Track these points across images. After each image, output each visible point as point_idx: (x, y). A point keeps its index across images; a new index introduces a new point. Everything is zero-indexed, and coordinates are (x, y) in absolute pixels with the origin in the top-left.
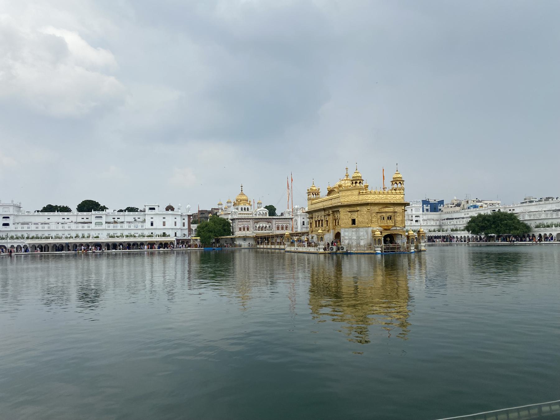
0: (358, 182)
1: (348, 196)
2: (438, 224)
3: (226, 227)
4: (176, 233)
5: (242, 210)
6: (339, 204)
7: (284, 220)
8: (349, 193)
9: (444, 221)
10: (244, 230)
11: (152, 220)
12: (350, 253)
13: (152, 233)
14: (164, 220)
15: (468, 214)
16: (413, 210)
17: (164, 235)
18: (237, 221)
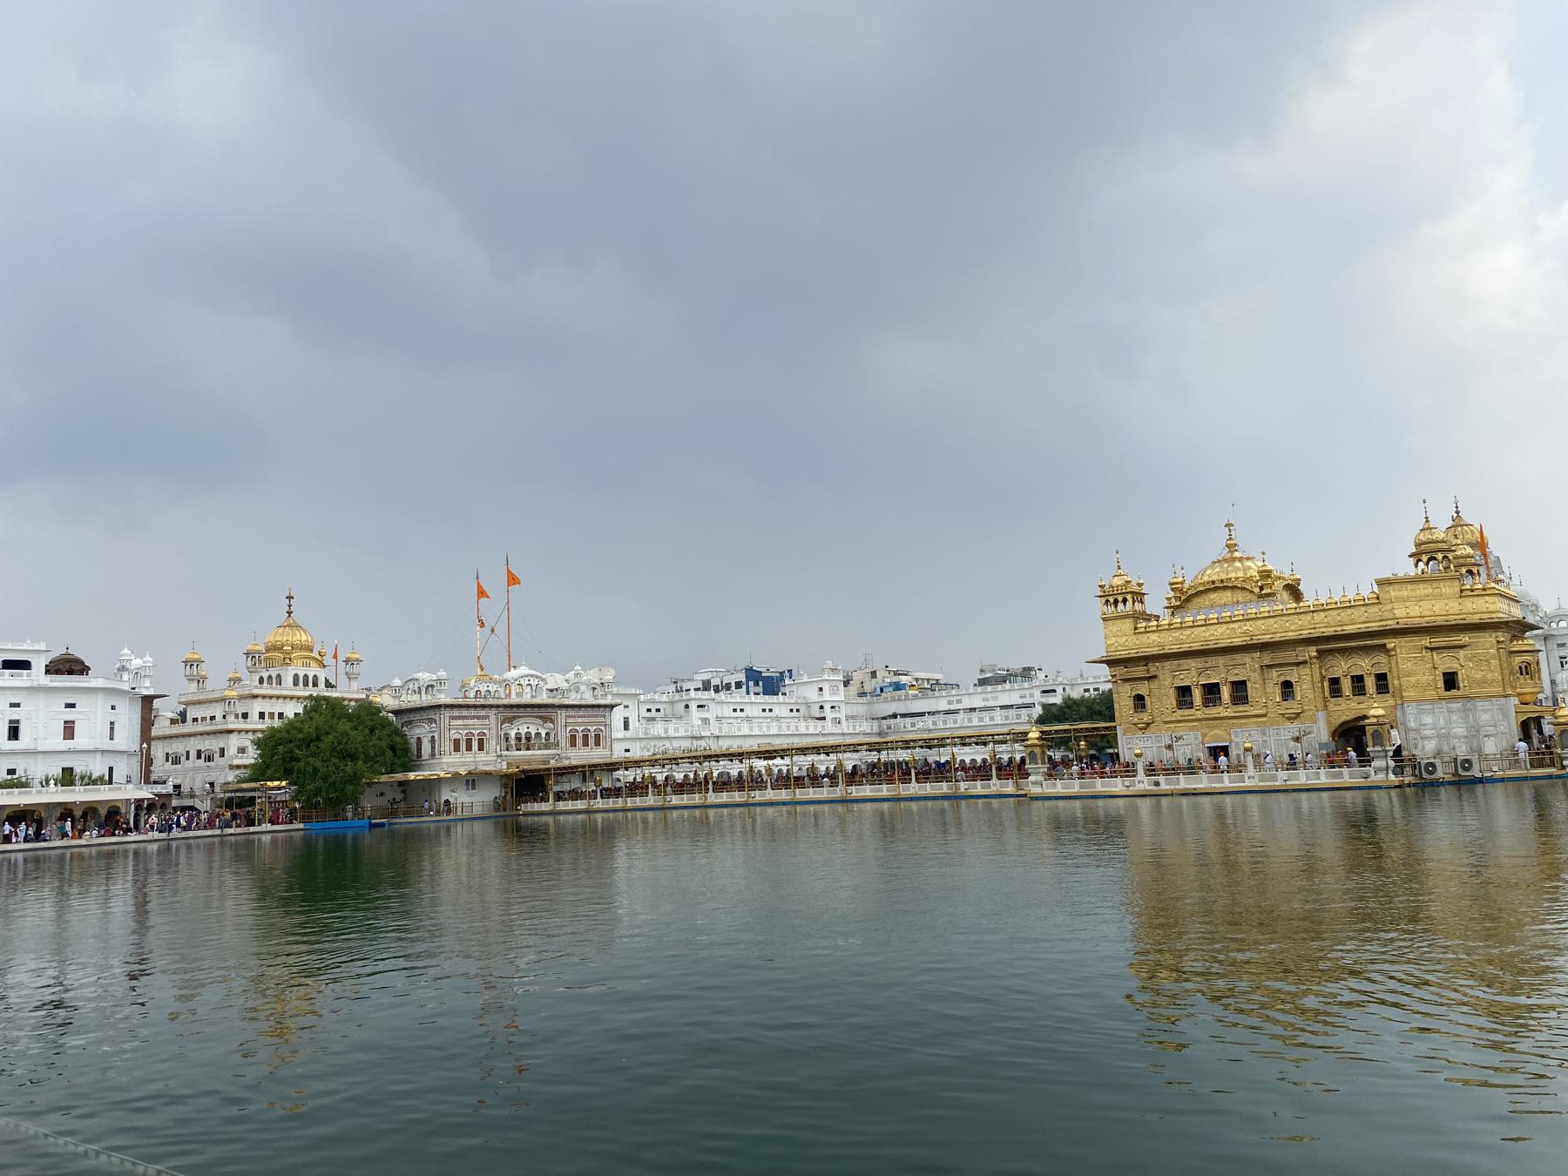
0: (1440, 556)
1: (1421, 599)
2: (876, 730)
3: (398, 739)
4: (111, 769)
5: (296, 683)
6: (1392, 624)
7: (591, 712)
8: (1423, 590)
9: (892, 721)
10: (469, 748)
11: (14, 714)
12: (1491, 780)
13: (11, 772)
14: (70, 715)
15: (959, 701)
16: (826, 687)
17: (68, 778)
18: (448, 713)
